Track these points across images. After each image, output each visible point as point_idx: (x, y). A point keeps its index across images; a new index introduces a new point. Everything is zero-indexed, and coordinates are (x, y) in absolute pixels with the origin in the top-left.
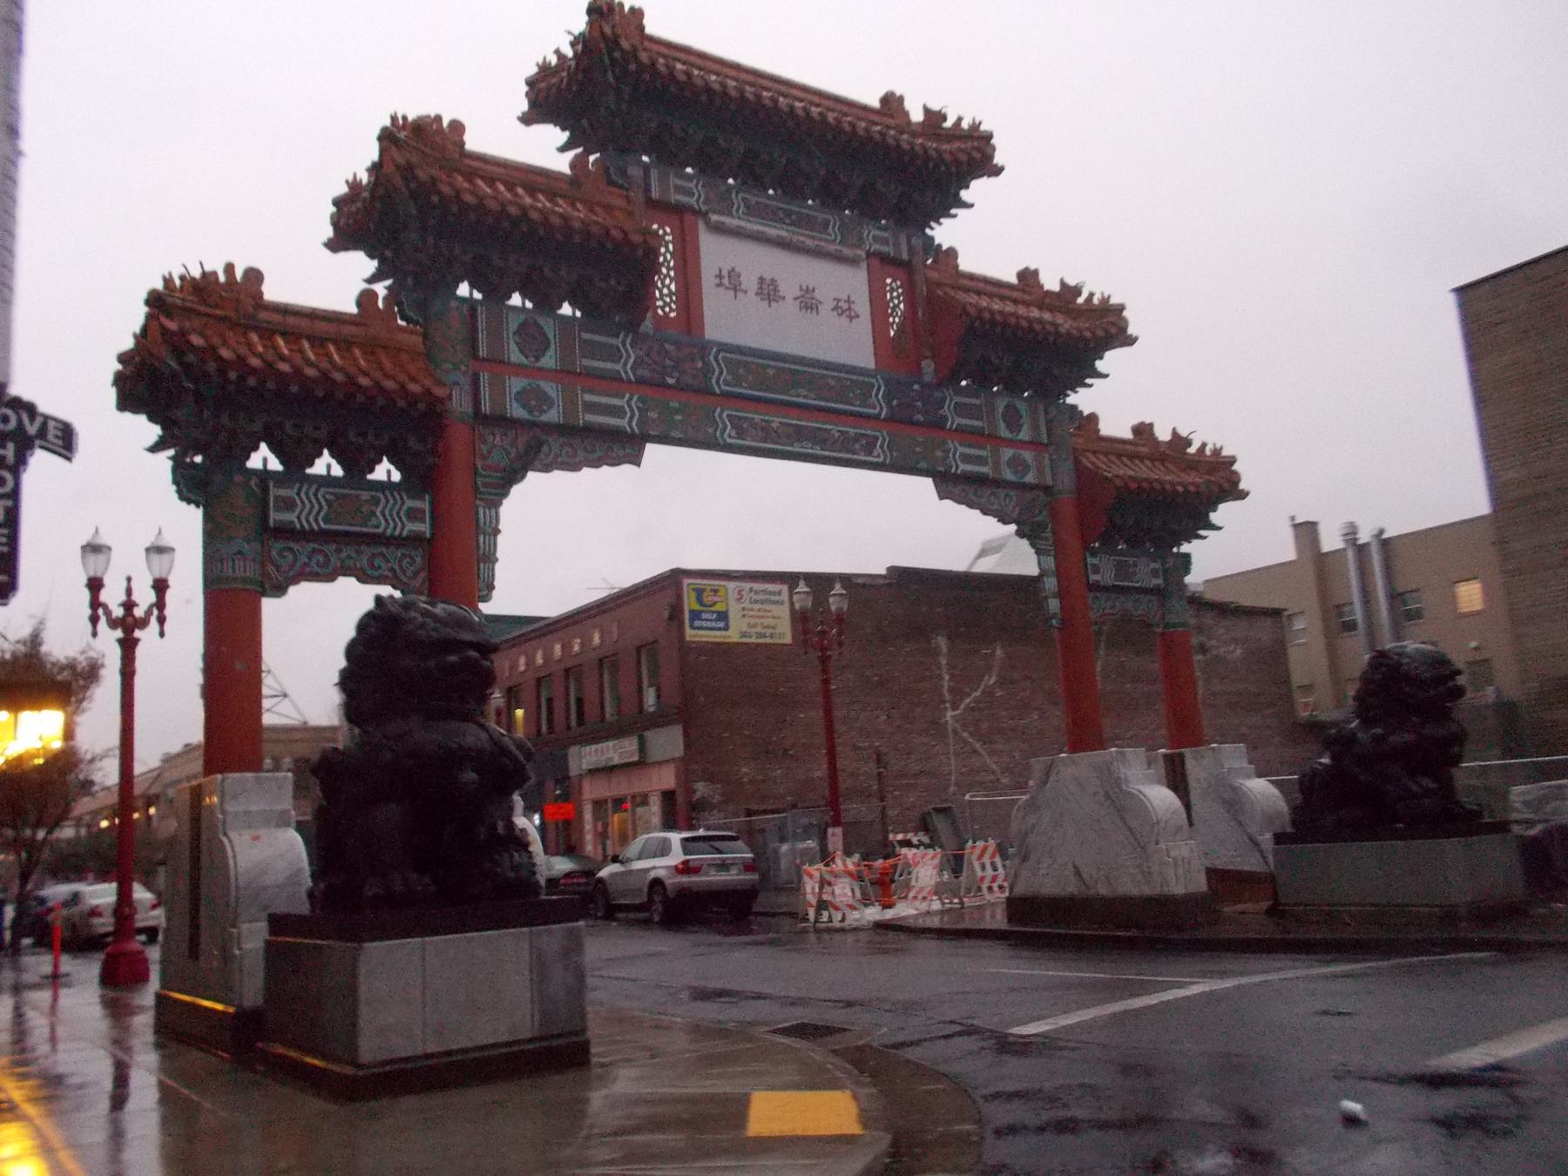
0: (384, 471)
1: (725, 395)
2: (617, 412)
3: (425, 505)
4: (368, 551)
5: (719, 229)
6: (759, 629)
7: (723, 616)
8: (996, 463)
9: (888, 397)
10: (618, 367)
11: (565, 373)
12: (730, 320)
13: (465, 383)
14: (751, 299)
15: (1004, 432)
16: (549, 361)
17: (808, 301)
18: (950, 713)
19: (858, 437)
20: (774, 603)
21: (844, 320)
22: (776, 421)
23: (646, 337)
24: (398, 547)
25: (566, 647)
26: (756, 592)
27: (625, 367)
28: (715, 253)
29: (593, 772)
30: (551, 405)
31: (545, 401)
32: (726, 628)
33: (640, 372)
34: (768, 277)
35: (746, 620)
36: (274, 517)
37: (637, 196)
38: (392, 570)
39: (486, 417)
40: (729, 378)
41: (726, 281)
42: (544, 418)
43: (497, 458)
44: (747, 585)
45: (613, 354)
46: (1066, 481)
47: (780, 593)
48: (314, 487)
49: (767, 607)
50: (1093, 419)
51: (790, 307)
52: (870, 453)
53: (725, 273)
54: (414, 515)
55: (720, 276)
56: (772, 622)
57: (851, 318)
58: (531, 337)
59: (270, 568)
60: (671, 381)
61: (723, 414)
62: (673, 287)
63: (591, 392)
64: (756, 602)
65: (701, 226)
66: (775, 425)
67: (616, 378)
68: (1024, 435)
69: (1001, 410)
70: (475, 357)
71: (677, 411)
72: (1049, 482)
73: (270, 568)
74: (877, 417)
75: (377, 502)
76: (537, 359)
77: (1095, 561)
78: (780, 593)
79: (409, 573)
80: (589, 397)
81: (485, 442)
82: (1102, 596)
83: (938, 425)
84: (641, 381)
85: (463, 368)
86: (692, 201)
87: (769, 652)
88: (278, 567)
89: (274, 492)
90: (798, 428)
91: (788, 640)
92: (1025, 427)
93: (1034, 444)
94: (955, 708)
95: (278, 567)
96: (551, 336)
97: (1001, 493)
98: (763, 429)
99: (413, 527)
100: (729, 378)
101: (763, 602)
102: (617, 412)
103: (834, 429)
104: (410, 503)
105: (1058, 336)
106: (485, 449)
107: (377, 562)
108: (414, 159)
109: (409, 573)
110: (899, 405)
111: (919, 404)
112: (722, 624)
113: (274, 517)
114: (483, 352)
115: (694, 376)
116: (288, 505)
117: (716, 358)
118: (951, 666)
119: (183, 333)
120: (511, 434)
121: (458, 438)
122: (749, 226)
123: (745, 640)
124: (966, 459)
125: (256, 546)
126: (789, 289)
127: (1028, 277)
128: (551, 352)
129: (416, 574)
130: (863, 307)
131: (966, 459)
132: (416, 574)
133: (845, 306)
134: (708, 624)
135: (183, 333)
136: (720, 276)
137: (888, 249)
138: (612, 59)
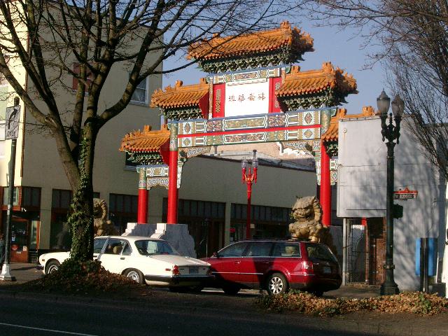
1: (226, 131)
2: (202, 141)
3: (167, 169)
11: (192, 135)
19: (257, 136)
27: (204, 130)
28: (229, 91)
68: (312, 123)
74: (264, 128)
90: (242, 136)
93: (315, 126)
102: (202, 141)
103: (252, 134)
116: (149, 172)
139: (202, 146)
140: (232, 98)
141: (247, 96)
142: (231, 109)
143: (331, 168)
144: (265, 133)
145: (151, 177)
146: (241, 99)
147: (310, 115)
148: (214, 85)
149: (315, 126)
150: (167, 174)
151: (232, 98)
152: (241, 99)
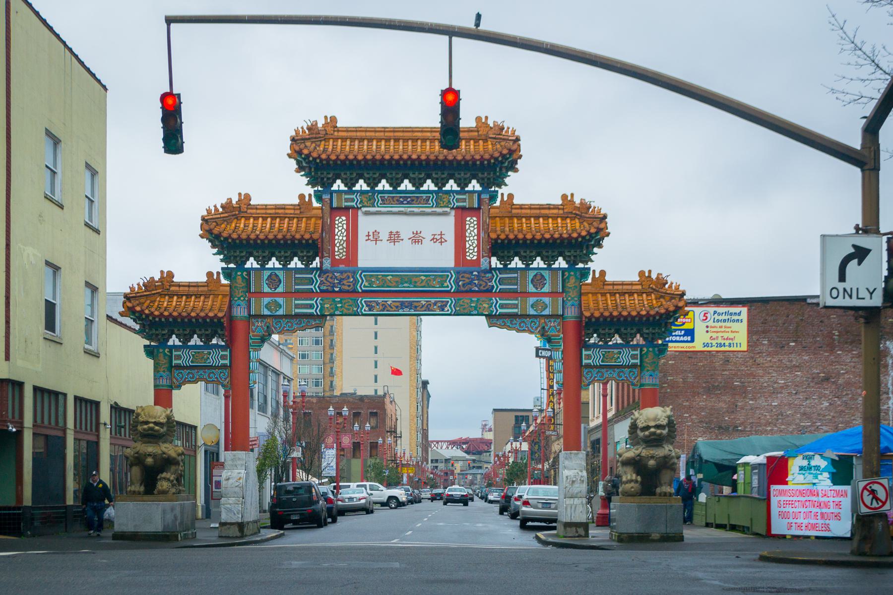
1: (364, 292)
2: (311, 306)
3: (227, 353)
5: (367, 213)
6: (720, 341)
7: (690, 333)
8: (524, 307)
9: (457, 282)
10: (312, 287)
12: (370, 256)
13: (244, 304)
14: (384, 244)
15: (531, 289)
16: (280, 289)
19: (435, 303)
20: (734, 321)
22: (390, 301)
26: (719, 314)
27: (315, 287)
28: (366, 224)
32: (692, 341)
33: (322, 288)
34: (394, 231)
35: (710, 334)
36: (175, 362)
37: (327, 209)
40: (367, 284)
41: (371, 237)
42: (278, 313)
44: (711, 310)
45: (311, 281)
46: (571, 313)
47: (739, 314)
49: (727, 324)
51: (407, 243)
52: (443, 310)
53: (371, 234)
54: (223, 357)
55: (369, 236)
56: (731, 335)
57: (441, 242)
58: (274, 280)
60: (337, 289)
64: (718, 321)
65: (360, 213)
67: (311, 291)
68: (546, 289)
69: (531, 278)
72: (560, 312)
74: (449, 292)
75: (210, 354)
77: (587, 353)
78: (739, 314)
80: (297, 302)
83: (489, 291)
84: (322, 291)
86: (353, 204)
87: (727, 358)
89: (174, 353)
90: (402, 303)
91: (744, 347)
93: (553, 294)
96: (282, 278)
99: (222, 362)
100: (367, 284)
101: (725, 321)
102: (311, 306)
103: (423, 301)
104: (222, 353)
105: (577, 234)
108: (212, 227)
110: (463, 285)
112: (689, 338)
113: (175, 362)
116: (179, 357)
119: (134, 307)
121: (240, 328)
123: (706, 349)
124: (502, 306)
125: (167, 373)
126: (406, 234)
128: (282, 285)
131: (502, 306)
134: (678, 338)
135: (134, 307)
136: (369, 236)
137: (466, 204)
138: (304, 159)
139: (310, 316)
140: (375, 237)
141: (406, 234)
142: (370, 256)
143: (585, 362)
145: (184, 368)
146: (394, 237)
147: (542, 276)
149: (553, 294)
150: (227, 362)
151: (375, 237)
152: (394, 237)
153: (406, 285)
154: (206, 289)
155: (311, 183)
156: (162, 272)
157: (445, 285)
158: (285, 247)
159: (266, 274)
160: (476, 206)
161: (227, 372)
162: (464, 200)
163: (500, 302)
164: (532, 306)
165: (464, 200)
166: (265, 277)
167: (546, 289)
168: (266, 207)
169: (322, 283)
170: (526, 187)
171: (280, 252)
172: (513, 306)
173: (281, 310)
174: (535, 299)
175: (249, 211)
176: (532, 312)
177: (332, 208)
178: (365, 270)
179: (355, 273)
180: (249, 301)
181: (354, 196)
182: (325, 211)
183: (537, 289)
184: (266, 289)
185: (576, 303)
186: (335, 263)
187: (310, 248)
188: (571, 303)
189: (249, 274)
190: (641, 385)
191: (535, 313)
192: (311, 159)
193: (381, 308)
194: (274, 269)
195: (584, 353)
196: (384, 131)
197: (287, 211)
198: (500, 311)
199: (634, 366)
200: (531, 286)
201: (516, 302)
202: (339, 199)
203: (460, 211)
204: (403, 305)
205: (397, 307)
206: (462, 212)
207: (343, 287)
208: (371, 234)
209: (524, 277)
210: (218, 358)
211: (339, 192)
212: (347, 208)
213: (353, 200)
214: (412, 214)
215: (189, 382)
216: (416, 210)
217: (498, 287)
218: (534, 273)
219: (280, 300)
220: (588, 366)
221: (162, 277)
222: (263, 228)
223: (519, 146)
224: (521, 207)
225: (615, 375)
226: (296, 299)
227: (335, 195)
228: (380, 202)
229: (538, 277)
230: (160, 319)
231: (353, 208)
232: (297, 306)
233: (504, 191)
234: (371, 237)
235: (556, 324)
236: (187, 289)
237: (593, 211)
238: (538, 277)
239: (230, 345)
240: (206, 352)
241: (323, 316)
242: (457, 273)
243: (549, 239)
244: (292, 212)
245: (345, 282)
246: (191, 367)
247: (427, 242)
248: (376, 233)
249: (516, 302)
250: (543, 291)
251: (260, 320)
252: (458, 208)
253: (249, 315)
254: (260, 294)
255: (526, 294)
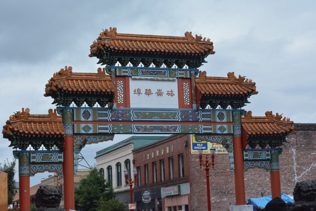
0: (54, 148)
1: (134, 121)
2: (107, 129)
3: (62, 155)
4: (50, 165)
5: (135, 79)
8: (215, 129)
9: (181, 116)
11: (94, 122)
12: (137, 102)
13: (71, 127)
14: (143, 96)
15: (218, 120)
16: (90, 119)
17: (159, 93)
18: (296, 177)
19: (172, 127)
21: (170, 96)
23: (115, 110)
24: (57, 164)
25: (155, 154)
27: (109, 118)
28: (133, 85)
29: (168, 197)
30: (90, 130)
31: (89, 128)
32: (206, 149)
34: (148, 89)
37: (113, 76)
38: (55, 169)
39: (76, 134)
41: (136, 92)
42: (89, 132)
43: (79, 142)
45: (106, 115)
46: (238, 132)
48: (39, 153)
50: (250, 112)
51: (154, 95)
52: (175, 131)
53: (136, 90)
54: (60, 157)
55: (135, 91)
57: (172, 95)
58: (86, 114)
59: (31, 171)
60: (120, 120)
61: (134, 126)
62: (122, 96)
63: (100, 125)
65: (130, 79)
66: (148, 127)
68: (225, 120)
69: (217, 114)
70: (73, 121)
71: (121, 127)
72: (232, 132)
73: (31, 171)
74: (178, 121)
75: (52, 155)
76: (88, 119)
77: (246, 153)
79: (59, 170)
80: (100, 126)
81: (75, 139)
82: (249, 163)
83: (197, 121)
84: (113, 121)
85: (70, 124)
86: (127, 74)
88: (33, 170)
89: (32, 155)
92: (225, 118)
93: (227, 123)
94: (298, 174)
95: (33, 170)
96: (91, 113)
97: (216, 137)
98: (144, 128)
102: (107, 129)
106: (76, 141)
107: (52, 168)
109: (59, 170)
110: (185, 117)
111: (191, 116)
112: (205, 148)
114: (75, 119)
115: (127, 118)
116: (34, 157)
117: (132, 112)
118: (297, 159)
119: (13, 129)
120: (82, 137)
121: (69, 140)
122: (143, 77)
124: (204, 129)
125: (28, 167)
126: (154, 91)
127: (231, 75)
129: (61, 170)
130: (176, 92)
131: (204, 129)
132: (61, 170)
133: (170, 93)
135: (13, 129)
136: (135, 91)
137: (184, 76)
138: (105, 49)
140: (138, 92)
141: (154, 91)
142: (137, 102)
143: (245, 158)
144: (179, 126)
146: (148, 92)
147: (223, 114)
148: (116, 76)
149: (227, 123)
151: (138, 92)
153: (156, 117)
154: (48, 119)
155: (102, 61)
156: (23, 109)
157: (176, 117)
158: (90, 96)
159: (82, 111)
160: (189, 77)
161: (61, 166)
162: (183, 74)
163: (203, 127)
164: (219, 129)
165: (183, 74)
166: (82, 113)
167: (225, 120)
168: (81, 74)
169: (112, 116)
170: (211, 68)
171: (106, 99)
172: (209, 129)
173: (91, 130)
174: (220, 125)
175: (72, 76)
176: (219, 132)
177: (116, 76)
178: (134, 109)
179: (129, 111)
180: (73, 126)
181: (127, 70)
182: (113, 77)
183: (220, 121)
184: (83, 119)
185: (240, 128)
186: (118, 105)
187: (107, 97)
188: (238, 128)
189: (73, 111)
190: (271, 170)
191: (220, 133)
192: (109, 49)
193: (144, 130)
194: (85, 108)
195: (245, 153)
196: (141, 37)
197: (93, 77)
198: (204, 131)
199: (268, 160)
200: (217, 118)
201: (211, 127)
202: (120, 71)
203: (180, 80)
204: (155, 128)
205: (152, 129)
206: (182, 79)
207: (124, 118)
208: (136, 90)
209: (214, 115)
210: (57, 158)
211: (118, 67)
212: (124, 76)
213: (127, 72)
214: (158, 80)
215: (40, 172)
216: (159, 78)
217: (201, 119)
218: (219, 112)
219: (91, 125)
220: (247, 160)
221: (23, 112)
222: (83, 86)
223: (213, 47)
224: (210, 78)
225: (259, 165)
226: (99, 125)
227: (117, 69)
228: (141, 73)
229: (221, 114)
230: (28, 136)
231: (127, 76)
232: (100, 129)
233: (201, 69)
234: (136, 92)
235: (230, 138)
236: (38, 118)
237: (246, 81)
238: (221, 114)
239: (62, 149)
240: (50, 154)
241: (113, 134)
242: (181, 111)
243: (225, 95)
244: (95, 77)
245: (124, 116)
246: (41, 163)
247: (165, 95)
248: (139, 90)
249: (211, 127)
250: (223, 121)
251: (79, 136)
252: (180, 78)
253: (74, 133)
254: (79, 122)
255: (215, 123)
